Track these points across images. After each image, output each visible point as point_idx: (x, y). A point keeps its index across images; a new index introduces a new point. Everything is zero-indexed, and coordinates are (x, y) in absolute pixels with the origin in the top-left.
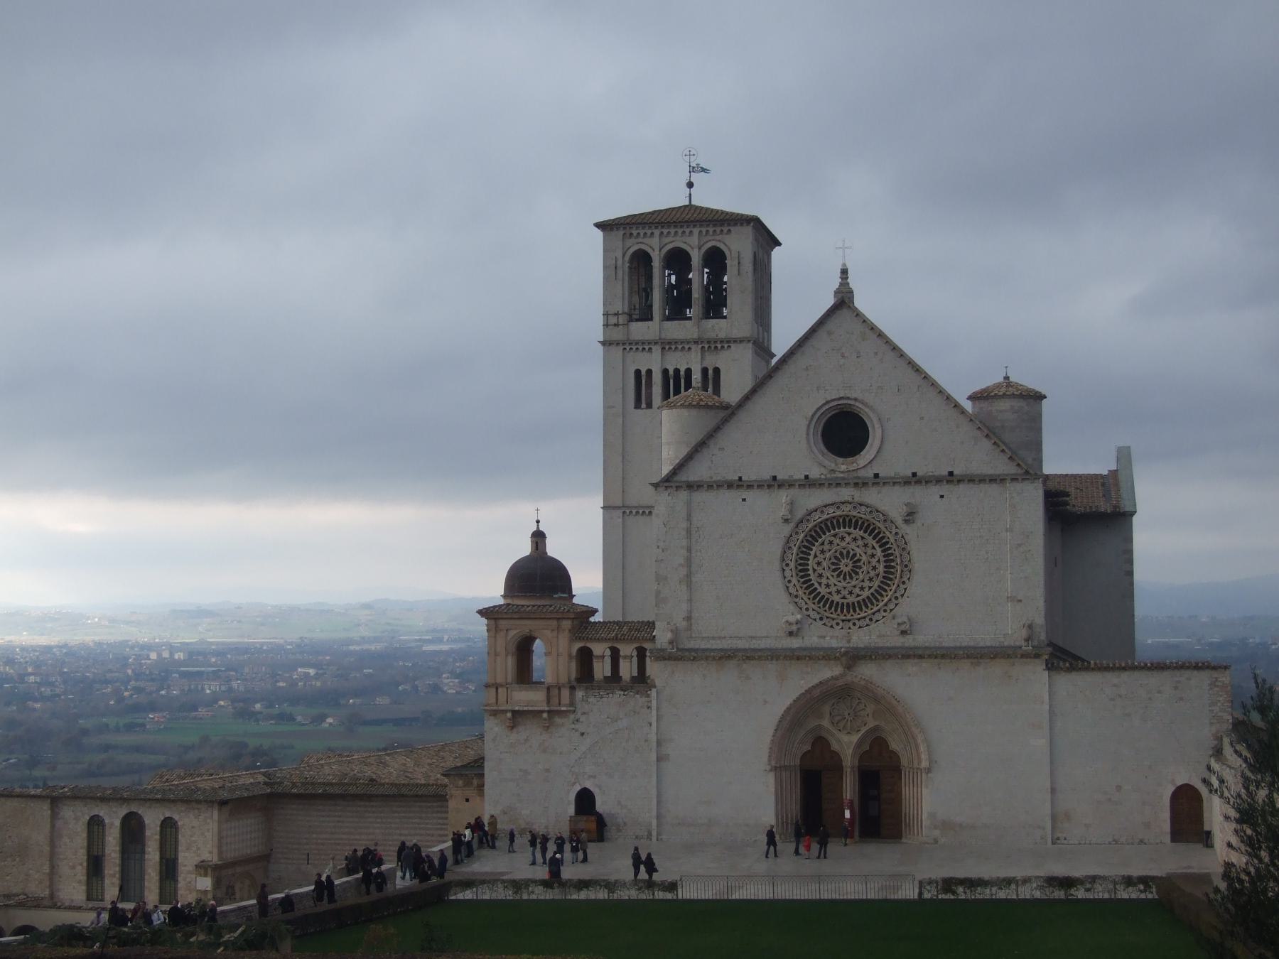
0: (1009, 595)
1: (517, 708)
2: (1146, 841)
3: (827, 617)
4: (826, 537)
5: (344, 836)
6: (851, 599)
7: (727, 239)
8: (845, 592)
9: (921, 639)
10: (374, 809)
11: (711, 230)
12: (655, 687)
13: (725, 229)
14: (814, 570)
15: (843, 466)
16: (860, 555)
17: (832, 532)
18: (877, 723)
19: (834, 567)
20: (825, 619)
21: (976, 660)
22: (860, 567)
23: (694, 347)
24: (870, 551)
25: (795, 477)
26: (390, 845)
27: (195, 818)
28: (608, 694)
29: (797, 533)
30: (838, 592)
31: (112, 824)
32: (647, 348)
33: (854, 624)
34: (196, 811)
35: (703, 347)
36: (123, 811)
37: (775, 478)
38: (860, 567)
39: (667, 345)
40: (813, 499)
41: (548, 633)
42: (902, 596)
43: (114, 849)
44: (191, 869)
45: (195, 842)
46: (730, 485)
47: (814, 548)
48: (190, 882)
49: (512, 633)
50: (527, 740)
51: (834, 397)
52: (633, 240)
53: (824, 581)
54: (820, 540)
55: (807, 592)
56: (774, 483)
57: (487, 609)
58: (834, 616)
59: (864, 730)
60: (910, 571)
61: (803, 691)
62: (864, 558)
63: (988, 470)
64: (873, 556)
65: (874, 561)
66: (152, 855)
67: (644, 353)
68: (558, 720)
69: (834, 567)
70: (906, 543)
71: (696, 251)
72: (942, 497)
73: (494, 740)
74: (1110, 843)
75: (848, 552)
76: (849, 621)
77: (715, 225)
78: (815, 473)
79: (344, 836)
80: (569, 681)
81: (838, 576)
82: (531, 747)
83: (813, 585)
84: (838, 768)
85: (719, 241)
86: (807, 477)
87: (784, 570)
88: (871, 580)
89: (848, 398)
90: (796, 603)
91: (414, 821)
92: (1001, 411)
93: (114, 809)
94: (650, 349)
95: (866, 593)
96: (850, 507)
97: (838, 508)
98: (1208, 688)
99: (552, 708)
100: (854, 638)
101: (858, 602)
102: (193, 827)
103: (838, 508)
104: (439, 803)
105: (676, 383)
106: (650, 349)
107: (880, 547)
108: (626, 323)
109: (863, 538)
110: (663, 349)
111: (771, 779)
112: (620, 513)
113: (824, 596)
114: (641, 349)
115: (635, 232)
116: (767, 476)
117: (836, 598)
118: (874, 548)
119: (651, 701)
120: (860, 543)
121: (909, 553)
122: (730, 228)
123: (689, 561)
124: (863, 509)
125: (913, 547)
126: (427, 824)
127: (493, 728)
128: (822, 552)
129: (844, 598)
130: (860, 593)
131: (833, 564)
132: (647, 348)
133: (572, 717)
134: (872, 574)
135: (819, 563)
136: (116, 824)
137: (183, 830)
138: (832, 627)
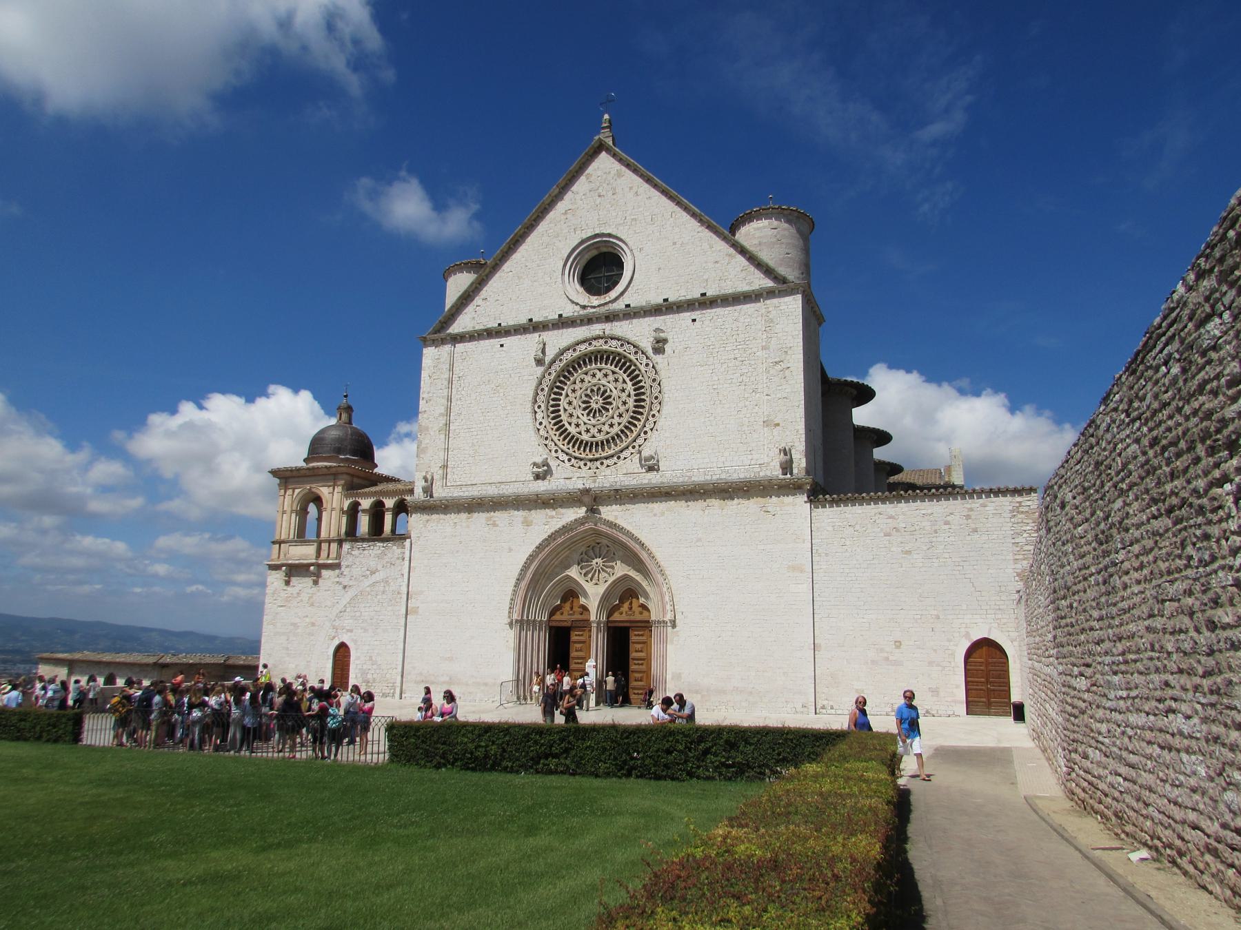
0: (765, 419)
1: (290, 562)
2: (934, 712)
3: (576, 458)
4: (577, 376)
6: (600, 437)
8: (594, 431)
9: (669, 474)
12: (410, 538)
14: (565, 410)
15: (595, 301)
16: (611, 391)
17: (584, 369)
18: (623, 573)
19: (584, 405)
20: (573, 460)
22: (610, 403)
24: (620, 386)
25: (550, 318)
30: (588, 431)
33: (602, 464)
37: (531, 320)
38: (610, 403)
42: (652, 430)
46: (490, 333)
47: (565, 387)
49: (297, 491)
51: (589, 234)
53: (574, 420)
54: (572, 379)
55: (558, 433)
56: (533, 327)
57: (286, 470)
58: (583, 456)
59: (611, 580)
60: (660, 403)
61: (545, 536)
63: (744, 287)
64: (623, 390)
65: (624, 396)
69: (584, 405)
70: (656, 373)
72: (694, 320)
73: (273, 594)
74: (887, 715)
75: (599, 389)
76: (597, 460)
78: (569, 311)
80: (339, 534)
81: (588, 415)
83: (564, 425)
84: (585, 625)
86: (560, 316)
87: (536, 412)
88: (620, 416)
90: (546, 445)
92: (758, 229)
95: (616, 429)
96: (602, 341)
97: (590, 344)
98: (1010, 515)
99: (321, 562)
100: (600, 479)
101: (608, 441)
103: (590, 344)
107: (631, 380)
109: (614, 373)
111: (511, 635)
113: (573, 437)
116: (523, 320)
117: (585, 437)
118: (624, 382)
120: (611, 378)
121: (659, 384)
124: (614, 343)
125: (663, 375)
127: (275, 580)
128: (574, 391)
129: (594, 437)
130: (609, 431)
131: (584, 402)
133: (337, 571)
134: (622, 409)
135: (570, 403)
138: (580, 468)
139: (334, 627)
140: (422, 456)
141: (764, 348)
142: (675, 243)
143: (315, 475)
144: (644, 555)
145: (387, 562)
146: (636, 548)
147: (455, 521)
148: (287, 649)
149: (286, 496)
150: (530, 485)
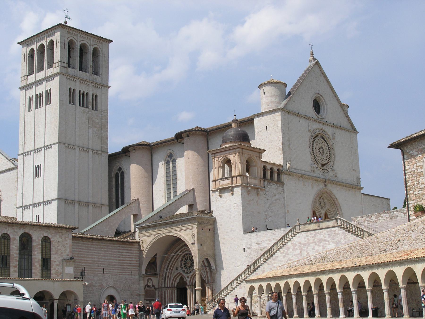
4: (316, 140)
5: (82, 259)
6: (323, 163)
7: (100, 45)
10: (94, 246)
11: (97, 40)
13: (101, 42)
21: (349, 188)
23: (90, 84)
26: (101, 264)
27: (60, 237)
28: (273, 185)
29: (311, 137)
31: (14, 239)
32: (75, 80)
33: (325, 171)
34: (61, 234)
35: (93, 85)
36: (21, 232)
39: (82, 81)
40: (315, 126)
41: (255, 157)
43: (16, 252)
44: (58, 263)
45: (60, 249)
48: (57, 270)
50: (253, 200)
52: (71, 36)
56: (306, 117)
62: (325, 149)
65: (327, 150)
66: (37, 256)
67: (73, 81)
68: (261, 193)
69: (319, 151)
71: (91, 46)
77: (98, 39)
78: (315, 117)
79: (82, 259)
82: (254, 202)
85: (98, 46)
89: (320, 94)
91: (109, 253)
93: (16, 231)
94: (76, 80)
95: (326, 161)
102: (59, 242)
104: (119, 245)
105: (83, 96)
106: (76, 80)
108: (68, 67)
110: (80, 82)
112: (64, 146)
114: (72, 79)
115: (71, 32)
117: (320, 161)
119: (284, 190)
122: (102, 42)
123: (289, 140)
126: (114, 254)
132: (75, 80)
133: (264, 192)
136: (17, 239)
137: (53, 243)
139: (266, 215)
140: (284, 154)
141: (352, 148)
142: (334, 106)
143: (254, 151)
144: (336, 202)
145: (279, 192)
146: (335, 199)
147: (296, 181)
148: (252, 221)
149: (236, 156)
150: (312, 174)
